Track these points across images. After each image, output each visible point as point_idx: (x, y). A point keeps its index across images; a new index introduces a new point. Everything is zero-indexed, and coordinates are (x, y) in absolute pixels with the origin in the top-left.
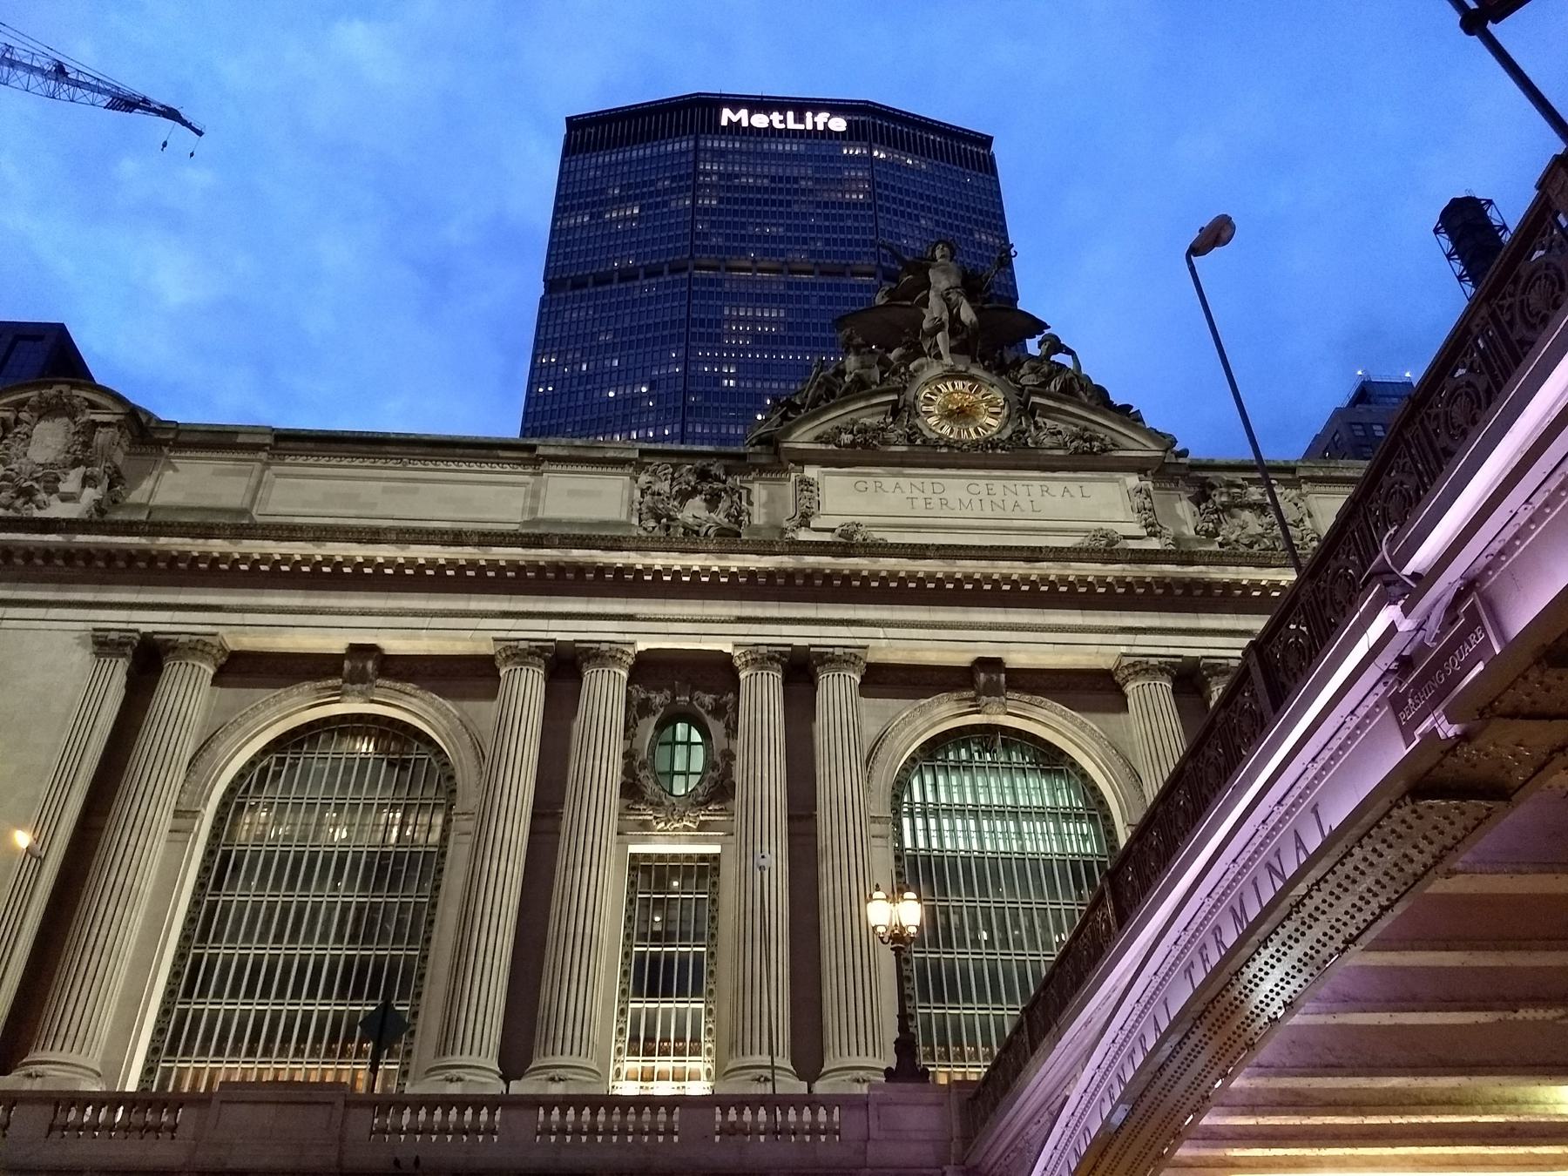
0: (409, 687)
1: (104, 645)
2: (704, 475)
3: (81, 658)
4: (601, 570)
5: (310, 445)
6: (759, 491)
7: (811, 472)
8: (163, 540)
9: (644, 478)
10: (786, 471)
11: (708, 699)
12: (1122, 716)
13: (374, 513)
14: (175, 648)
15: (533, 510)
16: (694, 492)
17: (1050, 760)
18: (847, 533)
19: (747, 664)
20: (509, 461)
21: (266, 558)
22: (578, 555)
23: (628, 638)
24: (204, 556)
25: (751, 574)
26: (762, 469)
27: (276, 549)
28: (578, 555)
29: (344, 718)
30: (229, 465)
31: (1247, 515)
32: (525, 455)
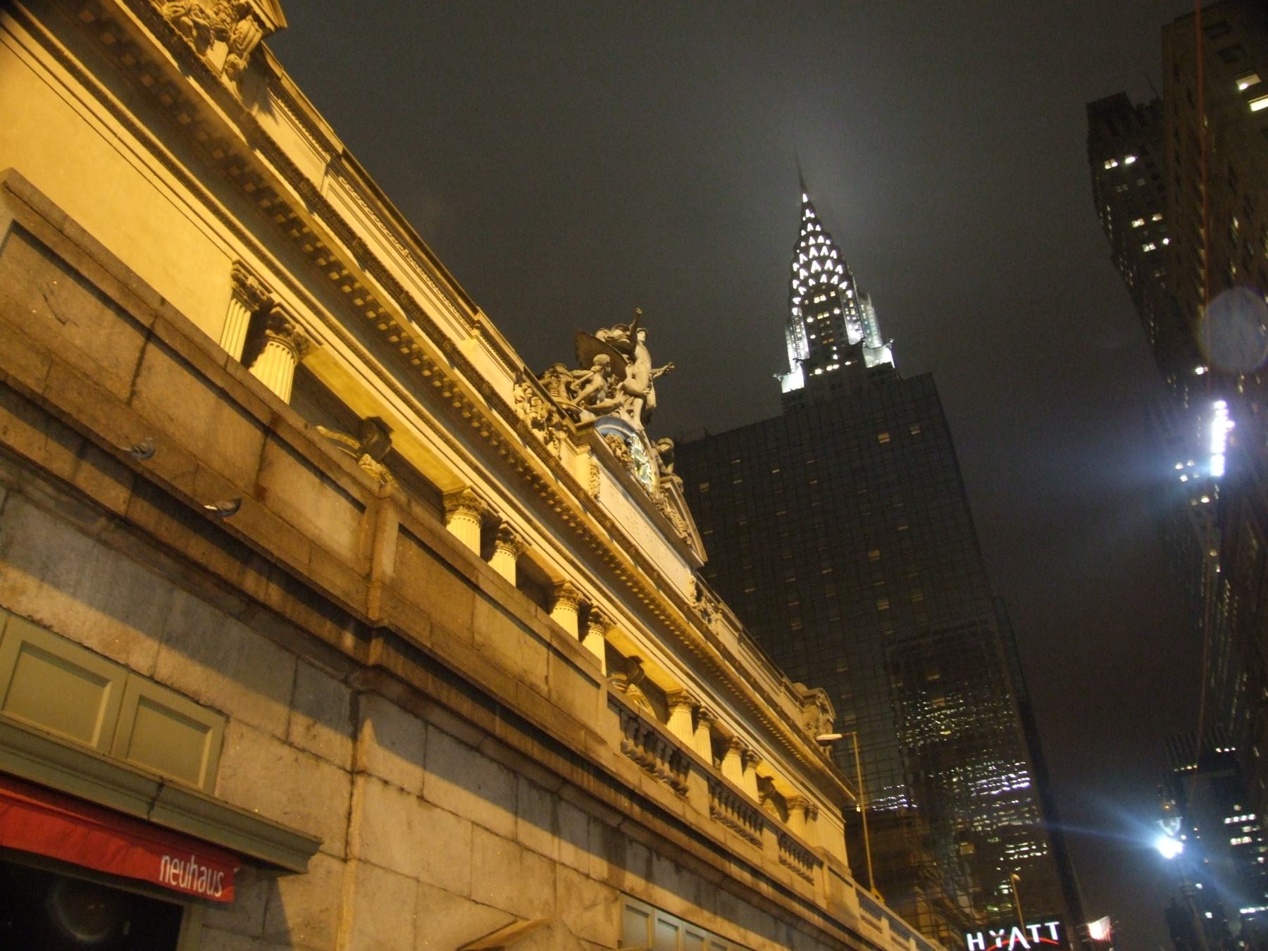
3: (225, 285)
10: (577, 446)
14: (288, 333)
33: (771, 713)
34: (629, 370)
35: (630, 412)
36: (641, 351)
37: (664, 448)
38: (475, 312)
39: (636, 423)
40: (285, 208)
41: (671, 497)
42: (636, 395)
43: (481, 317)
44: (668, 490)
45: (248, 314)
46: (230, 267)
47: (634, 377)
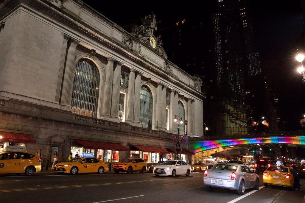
0: (97, 59)
1: (65, 37)
2: (130, 39)
3: (62, 37)
4: (123, 51)
5: (87, 8)
6: (134, 44)
7: (141, 45)
8: (76, 22)
9: (123, 36)
10: (137, 42)
11: (127, 74)
12: (156, 88)
13: (94, 25)
14: (74, 42)
15: (112, 35)
16: (128, 41)
17: (149, 91)
18: (143, 57)
19: (132, 71)
20: (109, 24)
21: (87, 31)
22: (122, 49)
23: (123, 63)
24: (80, 27)
25: (136, 59)
26: (135, 40)
27: (89, 30)
28: (122, 49)
29: (89, 60)
30: (76, 6)
31: (169, 68)
32: (112, 25)
33: (182, 84)
34: (152, 23)
35: (151, 32)
36: (154, 20)
37: (160, 37)
38: (113, 24)
39: (152, 34)
40: (72, 22)
41: (160, 47)
42: (152, 29)
43: (115, 25)
44: (159, 46)
45: (67, 41)
46: (63, 34)
47: (152, 25)
